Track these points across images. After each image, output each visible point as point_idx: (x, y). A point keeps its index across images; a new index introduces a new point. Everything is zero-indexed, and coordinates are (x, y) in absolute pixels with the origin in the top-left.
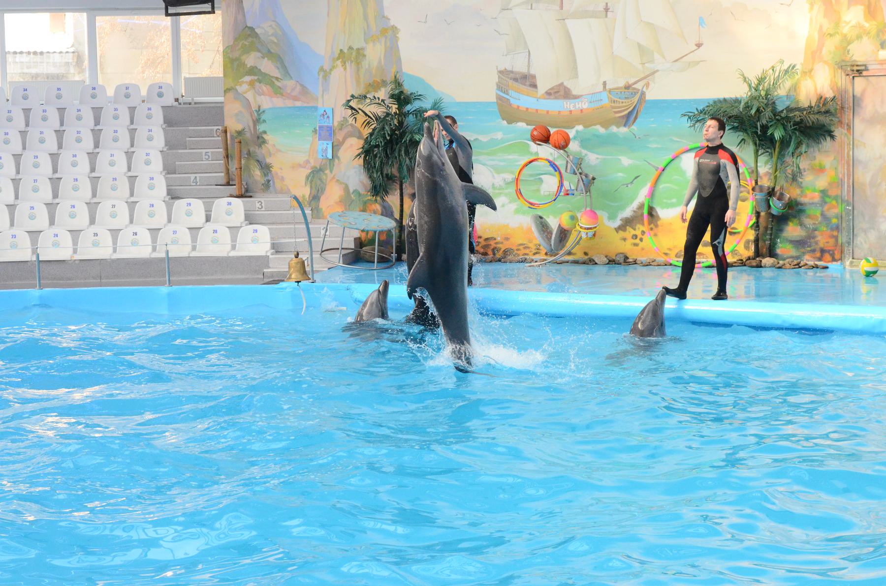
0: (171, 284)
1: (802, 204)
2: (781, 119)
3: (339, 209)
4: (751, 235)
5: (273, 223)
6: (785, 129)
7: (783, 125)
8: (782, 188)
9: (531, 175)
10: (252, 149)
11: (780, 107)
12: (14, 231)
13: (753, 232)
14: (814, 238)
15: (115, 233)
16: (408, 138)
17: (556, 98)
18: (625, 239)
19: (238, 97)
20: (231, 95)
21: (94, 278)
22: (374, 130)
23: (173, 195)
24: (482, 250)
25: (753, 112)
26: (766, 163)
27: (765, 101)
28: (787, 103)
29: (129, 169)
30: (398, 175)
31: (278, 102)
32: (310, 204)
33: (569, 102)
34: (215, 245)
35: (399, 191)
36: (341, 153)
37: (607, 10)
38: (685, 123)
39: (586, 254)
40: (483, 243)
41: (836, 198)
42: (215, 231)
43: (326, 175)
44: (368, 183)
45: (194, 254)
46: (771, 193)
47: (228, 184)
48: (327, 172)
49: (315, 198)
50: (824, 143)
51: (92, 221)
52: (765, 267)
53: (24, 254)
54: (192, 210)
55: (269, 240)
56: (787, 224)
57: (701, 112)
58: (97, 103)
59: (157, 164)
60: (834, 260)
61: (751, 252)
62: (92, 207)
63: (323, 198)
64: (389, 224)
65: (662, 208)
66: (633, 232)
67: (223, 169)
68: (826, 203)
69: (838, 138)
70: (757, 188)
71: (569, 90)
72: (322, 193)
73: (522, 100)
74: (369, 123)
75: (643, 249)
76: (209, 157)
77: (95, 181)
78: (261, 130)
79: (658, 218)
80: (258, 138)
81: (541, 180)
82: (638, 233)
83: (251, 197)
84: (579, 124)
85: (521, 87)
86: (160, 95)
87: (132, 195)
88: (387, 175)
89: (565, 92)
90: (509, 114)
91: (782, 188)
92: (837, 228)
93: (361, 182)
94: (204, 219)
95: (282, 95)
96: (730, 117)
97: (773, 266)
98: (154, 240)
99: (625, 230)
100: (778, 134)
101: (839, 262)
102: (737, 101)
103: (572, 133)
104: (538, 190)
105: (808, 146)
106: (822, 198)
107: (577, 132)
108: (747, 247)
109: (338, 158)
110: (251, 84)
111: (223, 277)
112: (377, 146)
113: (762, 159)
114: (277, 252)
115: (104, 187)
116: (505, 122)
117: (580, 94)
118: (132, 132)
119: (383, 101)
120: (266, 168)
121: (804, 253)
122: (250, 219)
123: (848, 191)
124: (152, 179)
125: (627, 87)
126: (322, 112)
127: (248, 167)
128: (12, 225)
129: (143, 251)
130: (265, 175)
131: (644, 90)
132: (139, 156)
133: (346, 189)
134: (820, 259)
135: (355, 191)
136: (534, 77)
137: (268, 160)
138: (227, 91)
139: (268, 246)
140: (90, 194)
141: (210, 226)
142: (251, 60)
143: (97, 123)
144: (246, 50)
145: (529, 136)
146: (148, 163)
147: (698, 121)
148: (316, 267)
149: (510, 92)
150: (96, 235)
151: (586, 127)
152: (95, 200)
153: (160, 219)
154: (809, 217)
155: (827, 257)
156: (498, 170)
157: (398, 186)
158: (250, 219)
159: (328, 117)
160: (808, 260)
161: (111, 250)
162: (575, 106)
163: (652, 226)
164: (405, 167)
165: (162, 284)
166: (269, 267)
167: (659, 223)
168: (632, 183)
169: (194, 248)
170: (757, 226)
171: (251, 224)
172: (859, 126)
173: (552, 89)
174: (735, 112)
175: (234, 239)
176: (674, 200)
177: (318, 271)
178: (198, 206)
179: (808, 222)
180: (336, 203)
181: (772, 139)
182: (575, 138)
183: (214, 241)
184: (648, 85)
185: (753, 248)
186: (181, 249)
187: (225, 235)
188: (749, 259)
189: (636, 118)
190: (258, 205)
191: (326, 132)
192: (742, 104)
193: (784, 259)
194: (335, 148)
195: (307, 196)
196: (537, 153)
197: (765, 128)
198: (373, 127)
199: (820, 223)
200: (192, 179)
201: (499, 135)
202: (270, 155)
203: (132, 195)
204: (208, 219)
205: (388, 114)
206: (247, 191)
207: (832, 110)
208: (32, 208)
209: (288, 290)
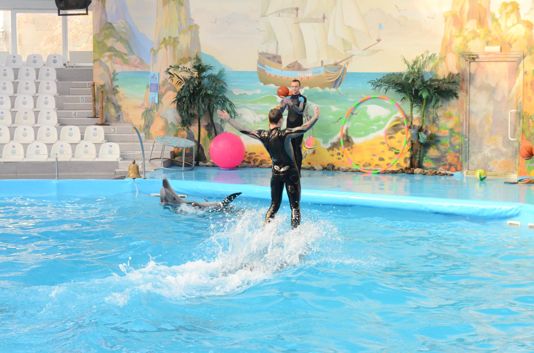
0: (59, 177)
1: (438, 137)
2: (426, 86)
3: (162, 134)
4: (408, 155)
5: (121, 142)
6: (429, 92)
7: (428, 89)
8: (427, 127)
10: (109, 96)
11: (426, 79)
13: (409, 153)
14: (445, 157)
15: (25, 146)
16: (204, 92)
17: (293, 70)
18: (333, 155)
19: (102, 64)
20: (97, 63)
21: (12, 173)
22: (183, 87)
23: (61, 123)
24: (247, 160)
25: (410, 81)
26: (418, 112)
27: (417, 75)
28: (431, 76)
29: (35, 107)
30: (197, 114)
31: (126, 68)
32: (144, 130)
34: (86, 154)
35: (197, 124)
36: (163, 100)
37: (324, 18)
38: (370, 87)
39: (309, 163)
40: (248, 156)
41: (458, 133)
42: (86, 146)
43: (154, 113)
44: (179, 118)
45: (73, 160)
46: (420, 130)
47: (95, 117)
48: (155, 111)
49: (147, 126)
50: (452, 101)
51: (12, 138)
52: (416, 174)
54: (73, 132)
55: (118, 152)
56: (429, 148)
58: (16, 66)
59: (52, 104)
60: (457, 170)
61: (408, 165)
62: (12, 130)
63: (152, 127)
64: (192, 144)
65: (356, 137)
66: (338, 151)
67: (92, 107)
68: (452, 136)
69: (460, 98)
70: (412, 127)
71: (301, 65)
72: (152, 123)
73: (273, 71)
74: (180, 82)
75: (343, 161)
76: (85, 99)
77: (14, 114)
78: (115, 85)
79: (353, 143)
80: (114, 89)
82: (341, 151)
83: (108, 125)
84: (306, 86)
85: (272, 63)
86: (55, 62)
87: (36, 122)
88: (191, 114)
89: (299, 67)
90: (265, 79)
91: (427, 127)
92: (459, 151)
93: (175, 118)
94: (79, 138)
95: (128, 64)
96: (396, 84)
97: (420, 173)
98: (49, 152)
99: (333, 150)
100: (425, 95)
101: (460, 172)
102: (401, 74)
105: (442, 103)
106: (450, 133)
107: (305, 90)
108: (405, 162)
109: (162, 103)
110: (110, 57)
111: (90, 174)
112: (185, 97)
113: (415, 109)
114: (124, 159)
115: (19, 117)
116: (262, 84)
117: (307, 68)
118: (37, 84)
119: (189, 69)
120: (118, 108)
121: (439, 166)
122: (108, 139)
123: (466, 130)
124: (49, 113)
125: (336, 64)
126: (152, 75)
127: (106, 106)
129: (43, 157)
130: (117, 112)
131: (346, 66)
132: (41, 99)
133: (166, 122)
134: (448, 170)
135: (171, 123)
136: (280, 57)
137: (119, 103)
138: (95, 61)
139: (118, 156)
140: (10, 121)
141: (83, 143)
142: (110, 42)
143: (16, 77)
144: (107, 37)
145: (276, 93)
146: (46, 103)
147: (377, 86)
148: (147, 169)
149: (266, 66)
150: (14, 147)
151: (310, 87)
152: (14, 125)
153: (53, 137)
154: (443, 144)
155: (453, 168)
156: (258, 112)
157: (197, 121)
158: (108, 139)
159: (156, 78)
161: (23, 157)
162: (304, 75)
163: (349, 148)
164: (201, 110)
165: (53, 177)
166: (118, 168)
167: (353, 146)
168: (337, 122)
169: (73, 156)
170: (412, 149)
171: (108, 141)
172: (472, 91)
174: (399, 82)
175: (98, 152)
176: (363, 133)
177: (148, 172)
178: (76, 130)
179: (442, 148)
180: (160, 130)
181: (421, 98)
183: (86, 152)
184: (348, 63)
185: (409, 162)
186: (66, 157)
187: (92, 149)
188: (406, 168)
189: (340, 83)
190: (113, 130)
191: (154, 87)
192: (404, 76)
193: (427, 169)
194: (160, 97)
195: (142, 126)
197: (417, 91)
198: (183, 85)
199: (449, 148)
200: (73, 113)
201: (259, 92)
202: (121, 100)
203: (36, 122)
204: (82, 138)
205: (192, 78)
206: (106, 121)
207: (457, 81)
209: (130, 183)
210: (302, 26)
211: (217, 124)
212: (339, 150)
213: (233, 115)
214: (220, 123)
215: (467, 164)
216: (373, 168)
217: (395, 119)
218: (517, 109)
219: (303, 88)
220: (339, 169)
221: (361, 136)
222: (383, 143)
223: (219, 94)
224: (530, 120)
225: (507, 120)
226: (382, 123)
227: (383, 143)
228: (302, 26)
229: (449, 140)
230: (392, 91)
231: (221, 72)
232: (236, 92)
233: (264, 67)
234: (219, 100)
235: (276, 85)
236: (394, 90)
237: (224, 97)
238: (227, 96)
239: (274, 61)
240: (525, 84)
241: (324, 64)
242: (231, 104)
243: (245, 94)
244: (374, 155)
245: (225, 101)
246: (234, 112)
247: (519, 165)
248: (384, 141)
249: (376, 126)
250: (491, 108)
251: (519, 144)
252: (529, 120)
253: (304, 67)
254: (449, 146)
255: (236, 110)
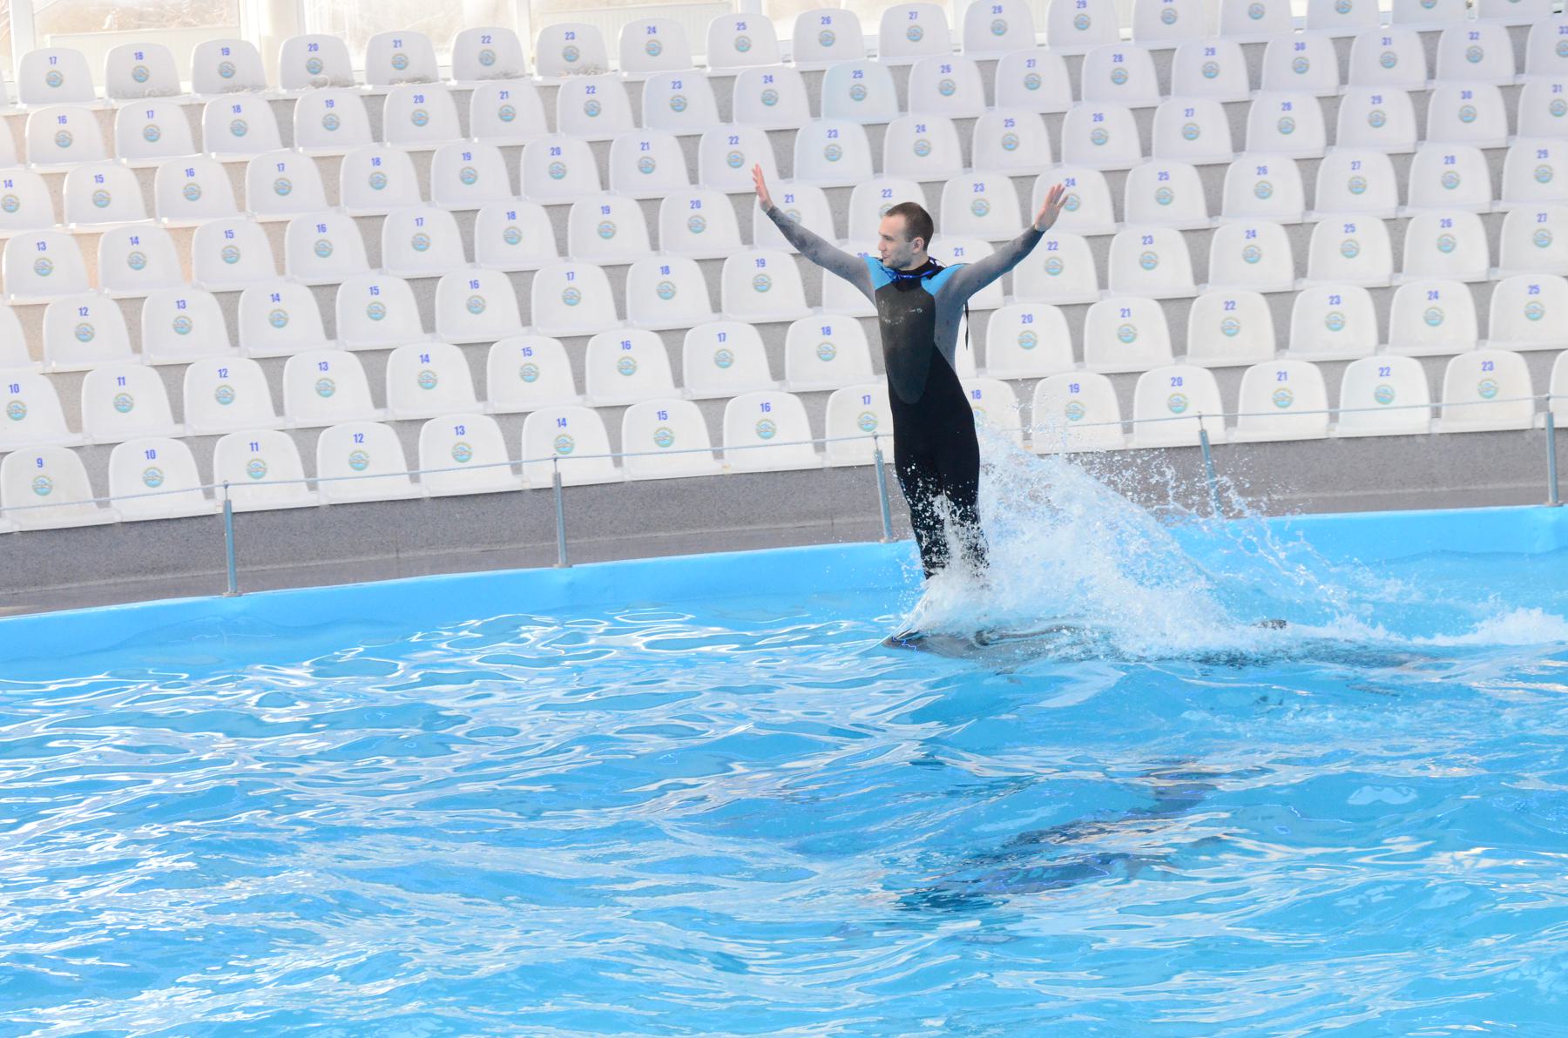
12: (1489, 351)
53: (1517, 413)
128: (1483, 333)
208: (1534, 289)
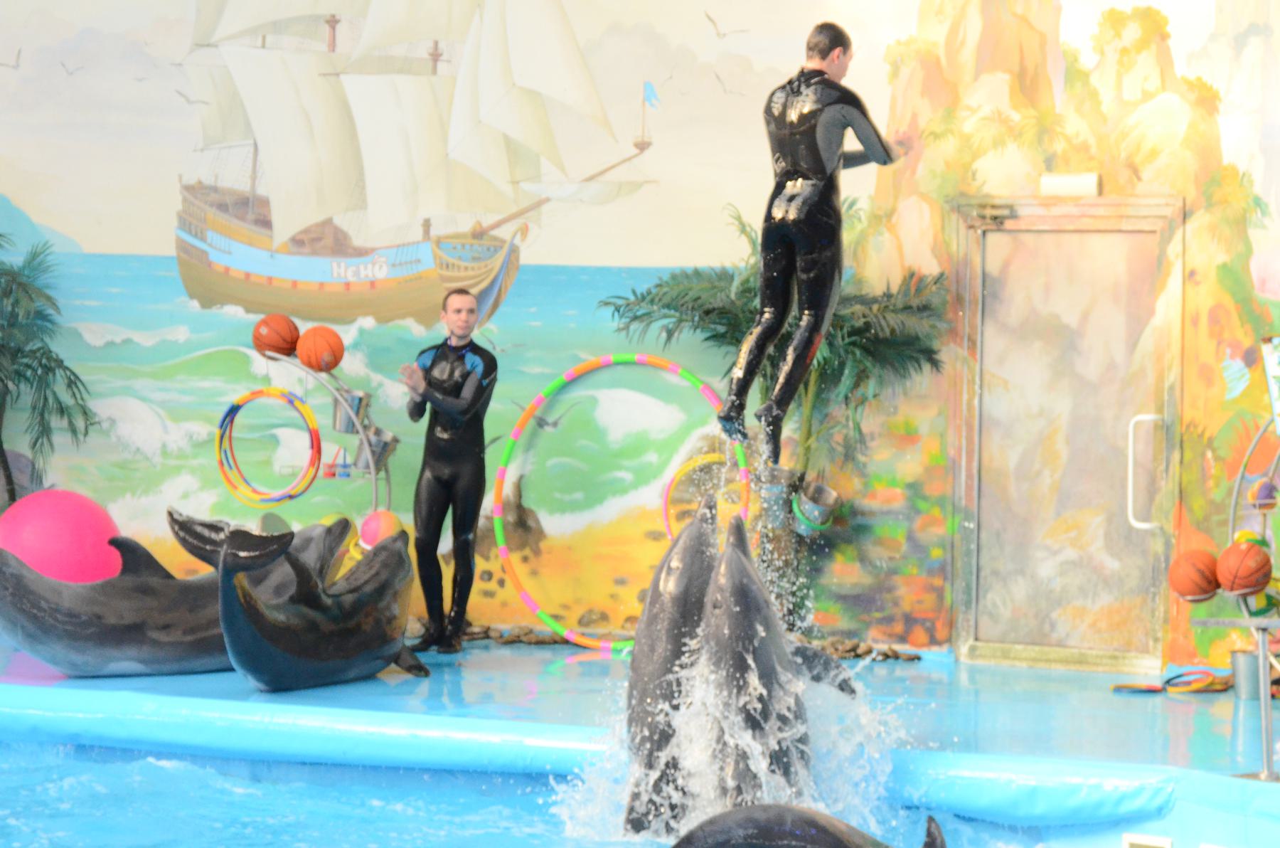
1: (863, 514)
8: (821, 475)
9: (252, 428)
14: (890, 590)
33: (343, 262)
37: (436, 56)
38: (609, 321)
46: (797, 485)
56: (830, 556)
57: (643, 298)
60: (933, 641)
65: (552, 511)
68: (918, 512)
69: (947, 368)
73: (237, 255)
75: (504, 604)
79: (541, 534)
81: (275, 440)
82: (494, 566)
84: (366, 314)
85: (236, 224)
90: (206, 286)
92: (943, 570)
96: (708, 312)
101: (945, 648)
102: (725, 276)
103: (348, 335)
104: (268, 463)
105: (881, 381)
107: (362, 332)
116: (195, 304)
117: (369, 245)
121: (868, 625)
125: (479, 234)
131: (517, 241)
134: (903, 639)
136: (265, 203)
145: (250, 339)
147: (635, 318)
149: (210, 235)
151: (382, 319)
155: (920, 634)
156: (176, 413)
160: (877, 641)
162: (357, 273)
163: (527, 552)
167: (543, 545)
172: (993, 340)
173: (306, 231)
174: (718, 301)
176: (578, 495)
179: (878, 554)
182: (356, 346)
184: (524, 231)
189: (496, 305)
196: (267, 379)
199: (904, 558)
201: (181, 334)
207: (935, 301)
210: (351, 84)
211: (19, 456)
212: (487, 558)
213: (80, 423)
214: (28, 453)
215: (972, 617)
216: (619, 631)
217: (700, 444)
218: (1160, 410)
219: (352, 321)
220: (486, 634)
221: (574, 507)
222: (656, 536)
223: (27, 341)
224: (1209, 454)
225: (1120, 453)
226: (652, 457)
227: (656, 536)
228: (351, 84)
229: (905, 525)
230: (691, 338)
231: (34, 255)
232: (94, 335)
233: (203, 239)
234: (28, 366)
235: (248, 311)
236: (700, 335)
237: (47, 353)
238: (58, 347)
239: (242, 218)
240: (1190, 320)
241: (434, 232)
242: (73, 382)
243: (127, 341)
244: (620, 582)
245: (48, 370)
246: (85, 413)
247: (1166, 621)
248: (660, 526)
249: (627, 469)
250: (1062, 406)
251: (1167, 544)
252: (1203, 455)
253: (357, 241)
254: (905, 547)
255: (92, 404)
